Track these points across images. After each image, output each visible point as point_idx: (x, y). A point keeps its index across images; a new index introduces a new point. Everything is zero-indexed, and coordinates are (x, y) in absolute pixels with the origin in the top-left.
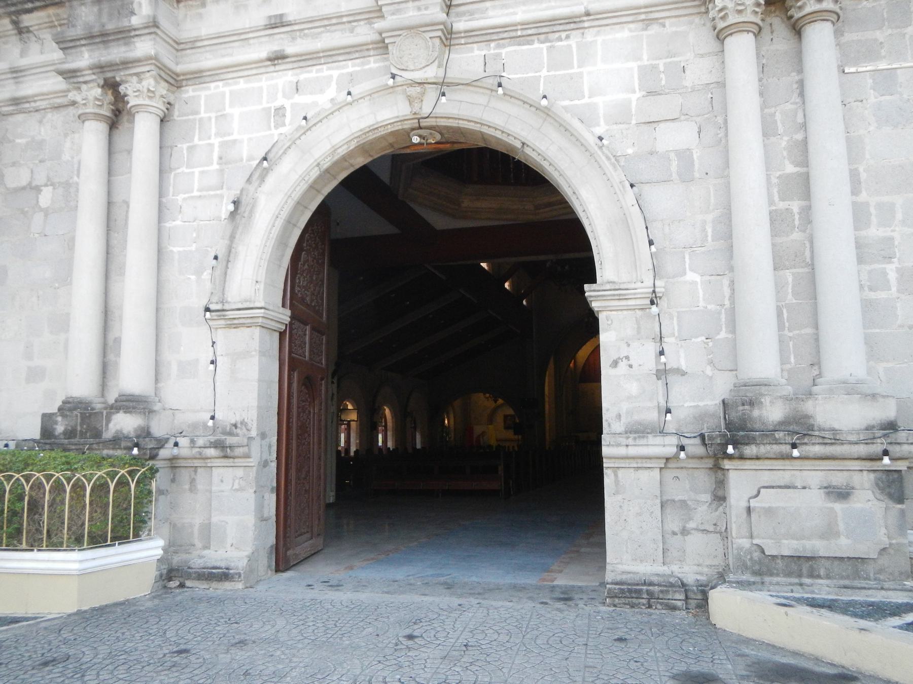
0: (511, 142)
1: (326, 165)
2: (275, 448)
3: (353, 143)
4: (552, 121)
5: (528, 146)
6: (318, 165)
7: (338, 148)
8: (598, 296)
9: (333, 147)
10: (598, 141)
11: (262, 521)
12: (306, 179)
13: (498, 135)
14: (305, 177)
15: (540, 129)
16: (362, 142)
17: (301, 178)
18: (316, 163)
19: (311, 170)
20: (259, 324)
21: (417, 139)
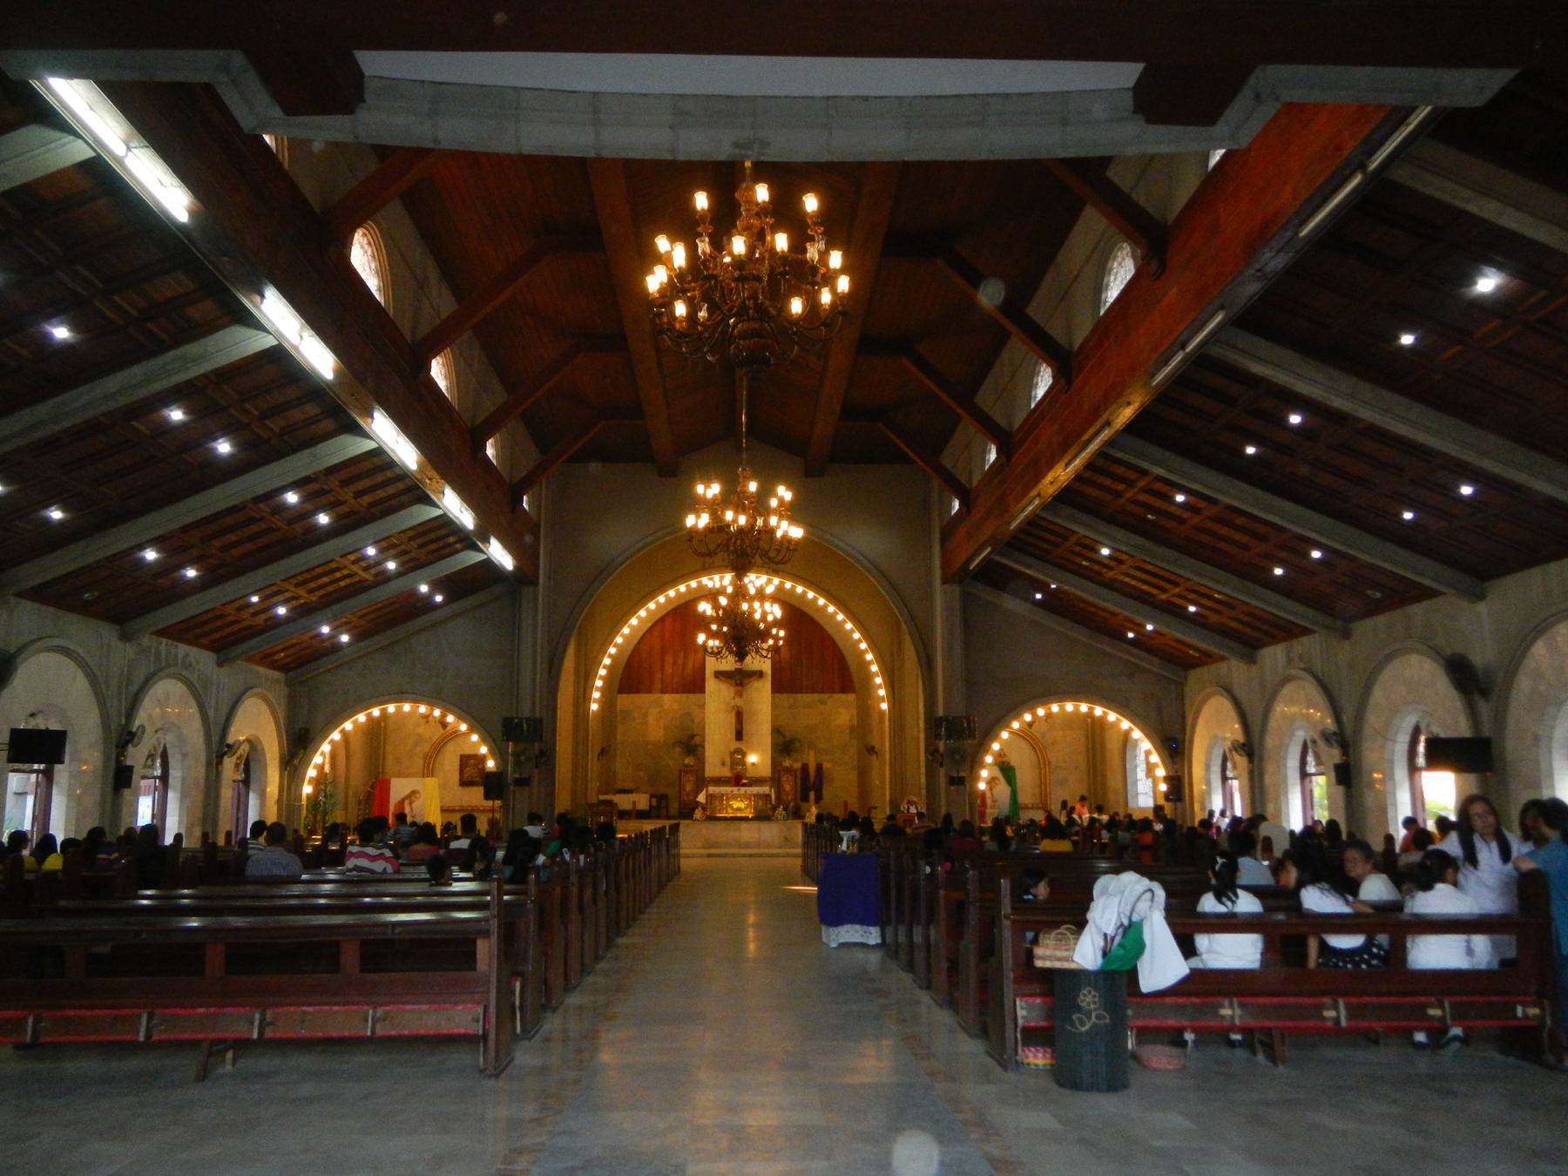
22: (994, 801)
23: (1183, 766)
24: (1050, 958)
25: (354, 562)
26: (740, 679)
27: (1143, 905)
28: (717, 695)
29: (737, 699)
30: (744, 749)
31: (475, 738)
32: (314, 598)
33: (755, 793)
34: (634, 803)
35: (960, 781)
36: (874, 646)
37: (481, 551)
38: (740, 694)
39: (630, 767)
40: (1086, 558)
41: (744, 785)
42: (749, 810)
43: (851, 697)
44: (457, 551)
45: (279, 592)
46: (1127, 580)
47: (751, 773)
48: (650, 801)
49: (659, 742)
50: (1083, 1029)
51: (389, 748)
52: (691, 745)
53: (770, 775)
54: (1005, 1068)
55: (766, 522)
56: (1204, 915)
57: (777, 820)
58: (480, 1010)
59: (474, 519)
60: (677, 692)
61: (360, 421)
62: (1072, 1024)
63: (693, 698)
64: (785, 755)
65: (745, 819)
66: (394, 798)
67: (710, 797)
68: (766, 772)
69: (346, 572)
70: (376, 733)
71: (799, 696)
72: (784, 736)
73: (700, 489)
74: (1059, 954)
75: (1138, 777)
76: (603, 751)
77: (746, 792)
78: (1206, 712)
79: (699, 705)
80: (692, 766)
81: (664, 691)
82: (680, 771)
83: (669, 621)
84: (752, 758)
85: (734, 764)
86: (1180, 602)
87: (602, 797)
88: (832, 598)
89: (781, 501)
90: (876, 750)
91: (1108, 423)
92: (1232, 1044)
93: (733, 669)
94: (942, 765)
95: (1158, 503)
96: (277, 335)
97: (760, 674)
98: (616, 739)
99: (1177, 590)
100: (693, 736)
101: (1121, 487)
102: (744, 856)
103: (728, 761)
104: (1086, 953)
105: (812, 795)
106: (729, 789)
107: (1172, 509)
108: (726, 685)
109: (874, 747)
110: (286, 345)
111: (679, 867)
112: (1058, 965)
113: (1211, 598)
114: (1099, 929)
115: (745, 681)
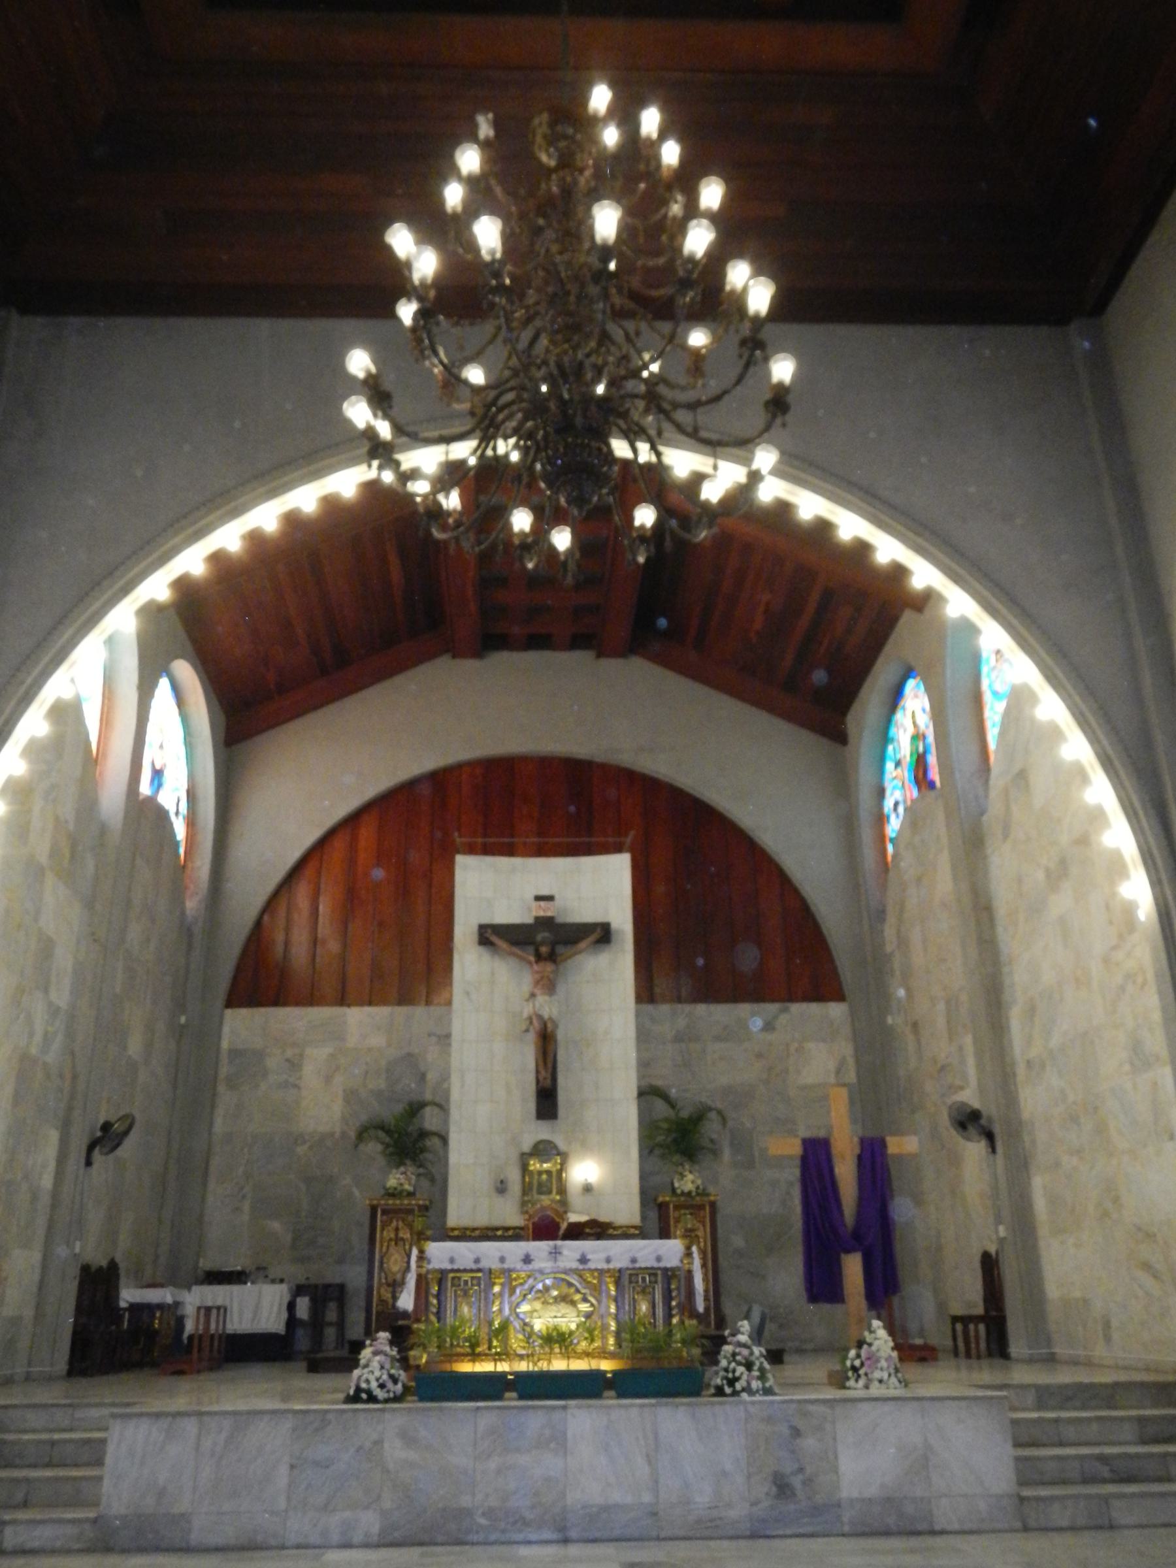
29: (541, 999)
30: (562, 1146)
33: (620, 1263)
38: (549, 986)
39: (246, 1206)
41: (576, 1232)
42: (596, 1344)
43: (836, 1010)
48: (291, 1306)
49: (332, 1134)
53: (636, 1220)
57: (727, 1389)
60: (384, 1002)
64: (677, 1158)
71: (701, 1009)
72: (672, 1104)
76: (106, 1127)
77: (583, 1260)
79: (439, 1037)
80: (411, 1195)
81: (342, 1000)
82: (374, 1209)
83: (367, 833)
85: (532, 1186)
87: (129, 1295)
90: (983, 1122)
93: (529, 920)
97: (602, 934)
98: (211, 1124)
103: (514, 1176)
105: (853, 1268)
106: (514, 1250)
108: (513, 962)
115: (560, 949)
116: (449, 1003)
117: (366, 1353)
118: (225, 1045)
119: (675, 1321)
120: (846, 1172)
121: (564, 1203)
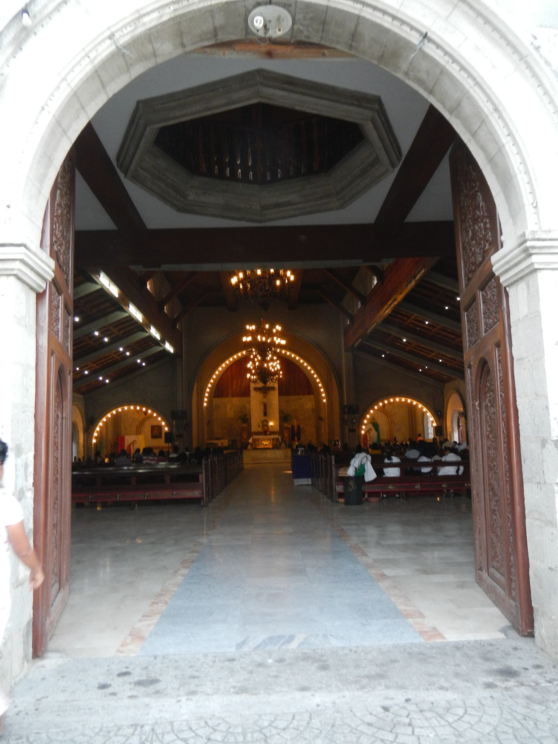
0: (403, 34)
1: (124, 38)
2: (31, 469)
3: (167, 10)
4: (466, 8)
5: (430, 40)
6: (111, 37)
7: (145, 15)
8: (544, 247)
9: (137, 11)
10: (532, 39)
11: (17, 586)
12: (92, 55)
13: (386, 22)
14: (91, 51)
15: (448, 17)
16: (180, 12)
17: (83, 54)
18: (108, 33)
19: (100, 43)
20: (15, 272)
21: (257, 22)
22: (371, 438)
23: (443, 422)
24: (342, 474)
25: (115, 353)
26: (265, 391)
27: (365, 460)
28: (255, 398)
30: (267, 419)
31: (159, 419)
32: (98, 367)
34: (222, 444)
35: (353, 431)
36: (320, 376)
37: (162, 346)
40: (399, 343)
41: (268, 435)
43: (312, 396)
44: (152, 347)
45: (87, 366)
46: (415, 350)
47: (270, 430)
48: (229, 443)
50: (350, 490)
51: (122, 424)
52: (245, 419)
53: (279, 430)
54: (333, 502)
55: (273, 339)
56: (385, 463)
58: (201, 492)
59: (160, 336)
61: (125, 308)
62: (348, 489)
63: (245, 399)
65: (269, 449)
66: (127, 443)
67: (254, 440)
68: (277, 429)
69: (111, 357)
70: (116, 419)
71: (290, 397)
73: (248, 327)
74: (344, 473)
75: (429, 427)
78: (451, 400)
82: (241, 430)
84: (271, 424)
86: (436, 358)
87: (208, 442)
88: (302, 357)
89: (277, 331)
91: (395, 300)
92: (397, 498)
93: (262, 386)
94: (346, 424)
95: (420, 324)
96: (102, 285)
97: (273, 388)
99: (434, 354)
100: (246, 415)
101: (406, 319)
102: (269, 463)
103: (261, 425)
104: (351, 472)
105: (296, 438)
107: (425, 326)
109: (321, 418)
110: (104, 288)
111: (243, 467)
112: (344, 475)
113: (447, 357)
114: (354, 466)
116: (250, 396)
117: (249, 446)
118: (214, 404)
119: (278, 443)
120: (296, 428)
121: (268, 428)
